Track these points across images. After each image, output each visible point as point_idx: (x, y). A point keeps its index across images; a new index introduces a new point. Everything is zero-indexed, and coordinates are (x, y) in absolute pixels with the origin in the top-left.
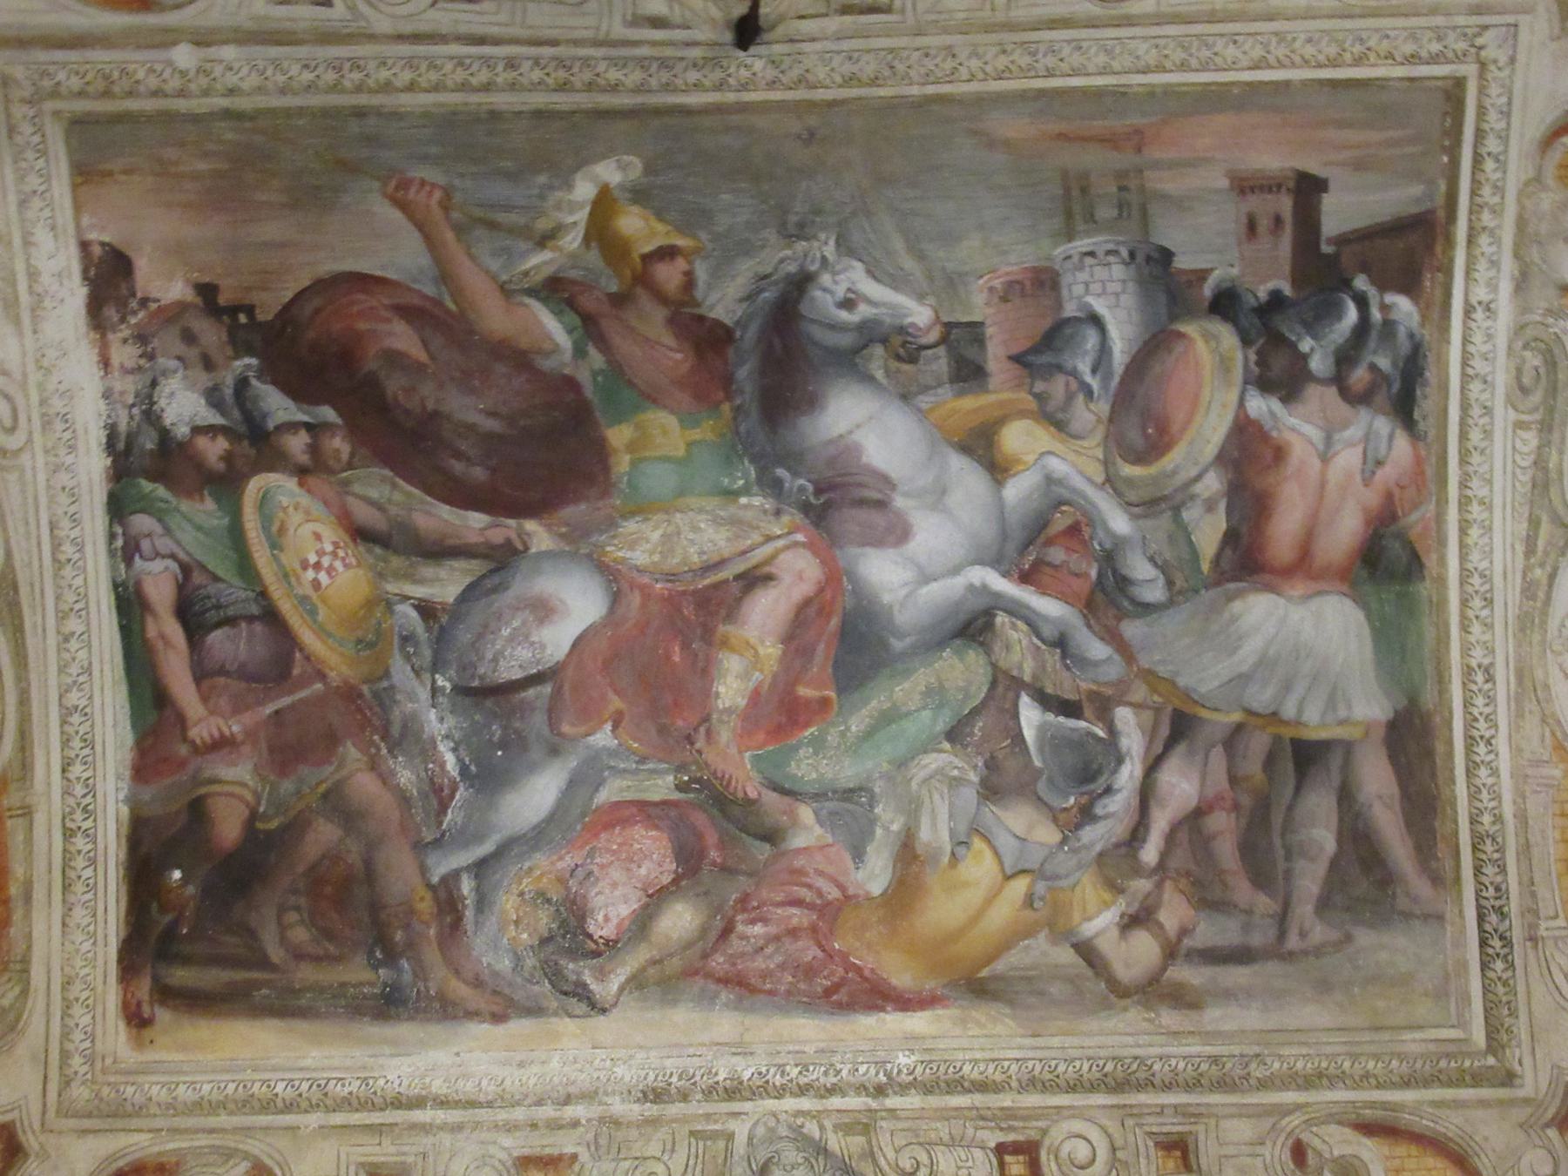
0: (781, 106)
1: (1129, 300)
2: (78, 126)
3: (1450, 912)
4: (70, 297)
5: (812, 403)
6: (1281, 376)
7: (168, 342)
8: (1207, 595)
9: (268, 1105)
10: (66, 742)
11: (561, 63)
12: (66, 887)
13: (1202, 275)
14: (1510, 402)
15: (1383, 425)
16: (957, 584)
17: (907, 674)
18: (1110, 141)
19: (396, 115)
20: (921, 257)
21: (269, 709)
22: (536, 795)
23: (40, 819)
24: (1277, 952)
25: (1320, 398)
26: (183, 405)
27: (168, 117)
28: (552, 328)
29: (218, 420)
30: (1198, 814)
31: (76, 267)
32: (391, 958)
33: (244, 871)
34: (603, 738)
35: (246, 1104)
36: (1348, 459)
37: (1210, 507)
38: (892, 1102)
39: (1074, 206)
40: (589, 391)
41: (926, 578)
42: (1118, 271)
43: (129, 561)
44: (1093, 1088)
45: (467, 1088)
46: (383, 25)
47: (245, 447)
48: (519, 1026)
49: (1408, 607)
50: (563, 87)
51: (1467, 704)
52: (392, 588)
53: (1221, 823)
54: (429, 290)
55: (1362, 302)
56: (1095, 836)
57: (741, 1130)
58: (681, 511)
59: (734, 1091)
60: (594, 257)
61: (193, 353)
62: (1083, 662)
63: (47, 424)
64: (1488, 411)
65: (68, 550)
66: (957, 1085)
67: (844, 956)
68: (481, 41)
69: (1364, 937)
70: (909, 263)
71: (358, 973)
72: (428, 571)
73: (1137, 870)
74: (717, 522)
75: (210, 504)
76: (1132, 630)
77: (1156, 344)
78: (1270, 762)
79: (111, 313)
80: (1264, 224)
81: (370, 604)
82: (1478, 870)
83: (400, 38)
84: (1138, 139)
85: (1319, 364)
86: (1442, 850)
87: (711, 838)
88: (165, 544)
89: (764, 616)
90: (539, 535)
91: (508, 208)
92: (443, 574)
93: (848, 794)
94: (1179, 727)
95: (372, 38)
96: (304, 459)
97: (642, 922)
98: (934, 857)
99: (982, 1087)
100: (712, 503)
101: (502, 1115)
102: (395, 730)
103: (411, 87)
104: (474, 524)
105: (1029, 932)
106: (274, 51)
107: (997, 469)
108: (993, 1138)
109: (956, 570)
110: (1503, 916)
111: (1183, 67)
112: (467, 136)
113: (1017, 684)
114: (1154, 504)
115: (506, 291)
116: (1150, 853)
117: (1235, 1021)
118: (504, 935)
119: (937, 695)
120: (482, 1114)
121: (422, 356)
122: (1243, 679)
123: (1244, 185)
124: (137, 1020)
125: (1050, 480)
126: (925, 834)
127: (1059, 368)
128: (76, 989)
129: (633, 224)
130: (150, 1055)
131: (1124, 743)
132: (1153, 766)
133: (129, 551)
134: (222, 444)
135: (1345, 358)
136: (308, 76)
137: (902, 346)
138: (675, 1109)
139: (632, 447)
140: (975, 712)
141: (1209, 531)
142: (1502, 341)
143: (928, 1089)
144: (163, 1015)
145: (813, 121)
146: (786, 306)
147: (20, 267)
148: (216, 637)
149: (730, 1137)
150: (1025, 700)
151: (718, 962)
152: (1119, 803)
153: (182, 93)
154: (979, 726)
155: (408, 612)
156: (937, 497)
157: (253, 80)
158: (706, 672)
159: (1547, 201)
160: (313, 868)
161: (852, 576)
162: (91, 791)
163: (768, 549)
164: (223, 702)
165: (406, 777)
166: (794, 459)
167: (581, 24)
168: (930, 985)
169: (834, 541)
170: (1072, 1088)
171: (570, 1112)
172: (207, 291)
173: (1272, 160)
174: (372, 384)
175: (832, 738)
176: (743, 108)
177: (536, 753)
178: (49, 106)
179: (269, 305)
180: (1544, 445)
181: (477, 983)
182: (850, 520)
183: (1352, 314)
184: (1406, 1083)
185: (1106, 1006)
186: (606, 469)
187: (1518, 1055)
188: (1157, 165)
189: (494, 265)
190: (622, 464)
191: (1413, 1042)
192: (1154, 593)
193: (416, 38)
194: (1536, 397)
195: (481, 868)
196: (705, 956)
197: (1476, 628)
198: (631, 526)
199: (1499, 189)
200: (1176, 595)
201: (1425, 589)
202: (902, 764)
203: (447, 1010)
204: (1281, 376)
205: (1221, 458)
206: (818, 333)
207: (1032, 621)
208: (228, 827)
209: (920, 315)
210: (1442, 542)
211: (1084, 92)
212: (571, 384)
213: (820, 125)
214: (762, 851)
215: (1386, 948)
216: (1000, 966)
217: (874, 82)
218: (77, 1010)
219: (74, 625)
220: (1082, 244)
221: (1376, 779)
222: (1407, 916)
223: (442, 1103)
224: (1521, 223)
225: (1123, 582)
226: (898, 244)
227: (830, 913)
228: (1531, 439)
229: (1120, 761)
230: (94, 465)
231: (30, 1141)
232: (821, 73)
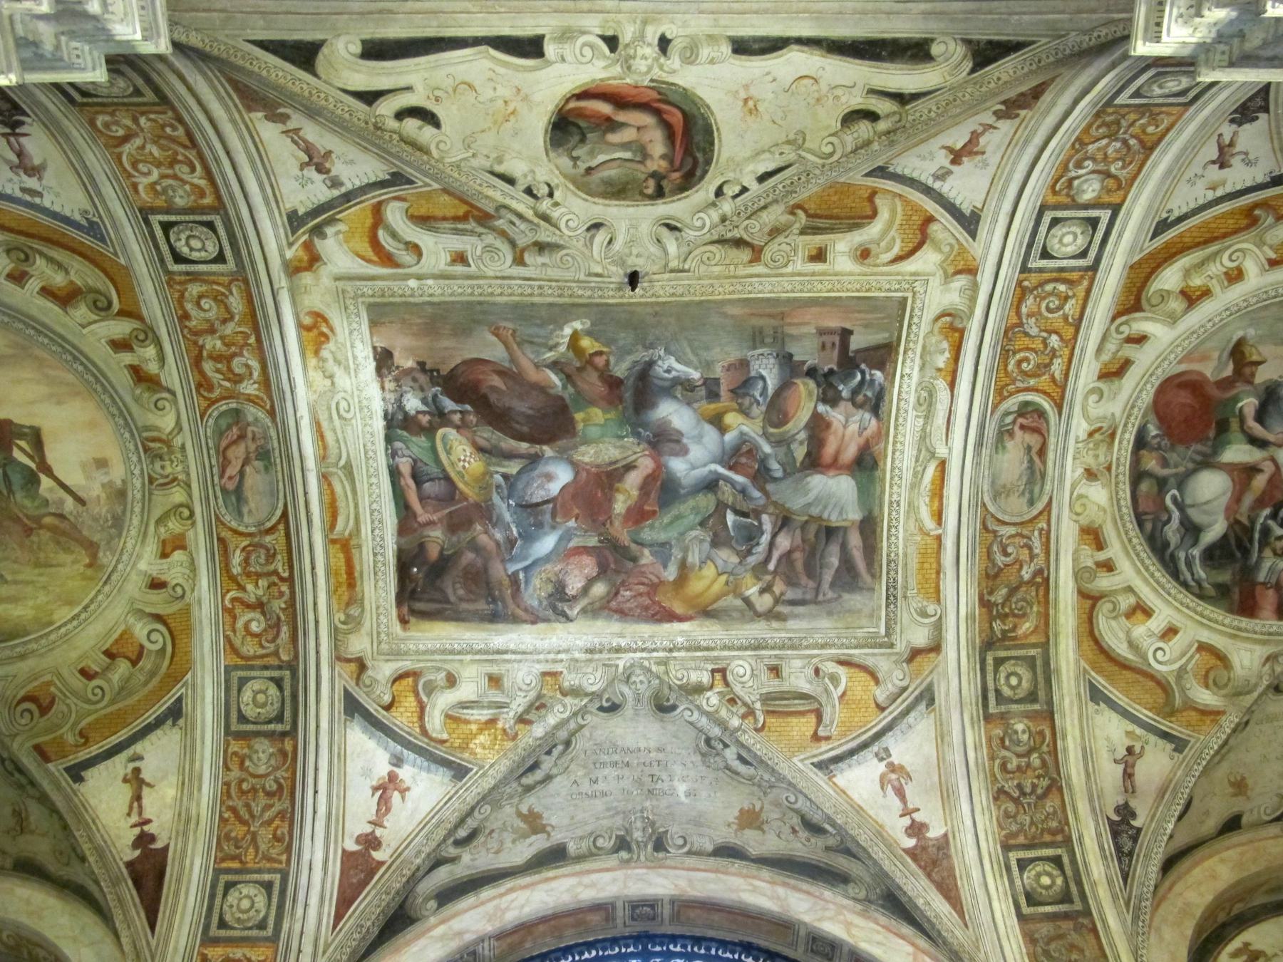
0: (646, 304)
1: (775, 371)
2: (371, 307)
3: (877, 587)
4: (369, 366)
5: (653, 405)
7: (407, 384)
8: (797, 475)
9: (452, 652)
10: (372, 522)
11: (559, 288)
12: (375, 574)
13: (804, 362)
14: (914, 408)
15: (867, 416)
16: (707, 469)
17: (684, 502)
18: (771, 316)
19: (494, 304)
20: (697, 355)
21: (447, 511)
22: (547, 543)
23: (364, 549)
24: (815, 602)
25: (845, 406)
26: (413, 403)
27: (406, 304)
28: (555, 379)
29: (424, 408)
30: (789, 554)
31: (371, 355)
32: (494, 601)
33: (440, 568)
34: (572, 523)
35: (444, 652)
36: (853, 427)
37: (801, 443)
38: (675, 654)
39: (757, 338)
40: (568, 401)
41: (694, 468)
42: (772, 360)
43: (393, 458)
44: (746, 649)
45: (523, 647)
46: (491, 274)
47: (437, 419)
48: (541, 626)
49: (871, 480)
50: (559, 296)
51: (890, 514)
52: (492, 469)
53: (798, 556)
54: (507, 364)
55: (863, 373)
56: (752, 560)
57: (621, 664)
58: (601, 441)
59: (618, 650)
60: (571, 354)
61: (416, 385)
62: (751, 499)
63: (361, 409)
64: (906, 411)
65: (371, 453)
66: (698, 648)
67: (659, 603)
68: (529, 279)
69: (846, 596)
70: (691, 356)
71: (481, 605)
72: (506, 463)
73: (767, 572)
74: (616, 447)
75: (423, 438)
76: (770, 487)
77: (784, 386)
78: (817, 535)
79: (385, 371)
80: (828, 345)
81: (484, 474)
82: (888, 573)
83: (497, 278)
84: (782, 316)
85: (845, 394)
86: (876, 566)
87: (611, 559)
88: (407, 452)
89: (633, 480)
90: (548, 451)
91: (538, 337)
92: (512, 463)
93: (663, 545)
94: (784, 522)
95: (485, 277)
96: (459, 423)
97: (585, 590)
98: (693, 566)
99: (708, 649)
100: (614, 440)
101: (536, 657)
102: (494, 519)
103: (501, 294)
104: (524, 446)
105: (725, 594)
106: (447, 282)
108: (710, 667)
109: (705, 465)
110: (895, 589)
111: (801, 291)
112: (524, 312)
113: (727, 506)
114: (780, 442)
115: (537, 366)
116: (771, 567)
117: (797, 626)
118: (536, 592)
119: (695, 510)
120: (529, 657)
121: (504, 388)
122: (809, 505)
123: (822, 332)
124: (404, 621)
125: (742, 434)
126: (690, 559)
127: (748, 394)
128: (381, 610)
129: (586, 343)
130: (408, 634)
131: (764, 527)
132: (774, 536)
133: (394, 454)
134: (427, 418)
135: (855, 392)
136: (460, 290)
137: (687, 386)
138: (597, 656)
139: (584, 420)
140: (710, 516)
141: (800, 452)
142: (913, 388)
143: (688, 649)
144: (413, 620)
145: (657, 309)
146: (644, 374)
147: (350, 354)
148: (427, 485)
149: (617, 666)
150: (729, 511)
151: (613, 604)
153: (412, 296)
155: (498, 478)
156: (699, 438)
157: (440, 291)
158: (610, 500)
159: (934, 340)
160: (465, 568)
161: (666, 467)
162: (382, 539)
163: (634, 457)
164: (430, 508)
165: (499, 536)
166: (645, 425)
167: (569, 275)
168: (690, 612)
169: (660, 454)
170: (739, 649)
171: (560, 656)
172: (422, 365)
173: (834, 323)
174: (485, 397)
175: (657, 524)
176: (630, 304)
177: (547, 528)
178: (360, 300)
179: (445, 370)
180: (925, 424)
181: (526, 610)
182: (668, 447)
183: (859, 377)
184: (856, 647)
185: (752, 620)
186: (574, 428)
187: (896, 638)
188: (790, 324)
189: (532, 356)
190: (580, 426)
191: (860, 633)
192: (779, 474)
193: (503, 278)
194: (924, 407)
195: (526, 569)
196: (608, 602)
197: (895, 488)
198: (583, 448)
199: (917, 335)
200: (787, 474)
201: (878, 473)
202: (682, 534)
203: (515, 620)
204: (831, 399)
205: (807, 426)
206: (656, 381)
207: (732, 483)
208: (433, 552)
209: (695, 375)
210: (886, 457)
211: (762, 299)
212: (562, 399)
213: (660, 310)
214: (630, 565)
215: (854, 600)
216: (715, 606)
217: (682, 295)
218: (382, 617)
219: (374, 480)
220: (760, 351)
221: (855, 540)
222: (861, 589)
223: (514, 652)
224: (924, 347)
225: (768, 470)
226: (688, 350)
227: (655, 587)
228: (921, 421)
229: (762, 533)
230: (379, 425)
231: (369, 663)
232: (661, 293)
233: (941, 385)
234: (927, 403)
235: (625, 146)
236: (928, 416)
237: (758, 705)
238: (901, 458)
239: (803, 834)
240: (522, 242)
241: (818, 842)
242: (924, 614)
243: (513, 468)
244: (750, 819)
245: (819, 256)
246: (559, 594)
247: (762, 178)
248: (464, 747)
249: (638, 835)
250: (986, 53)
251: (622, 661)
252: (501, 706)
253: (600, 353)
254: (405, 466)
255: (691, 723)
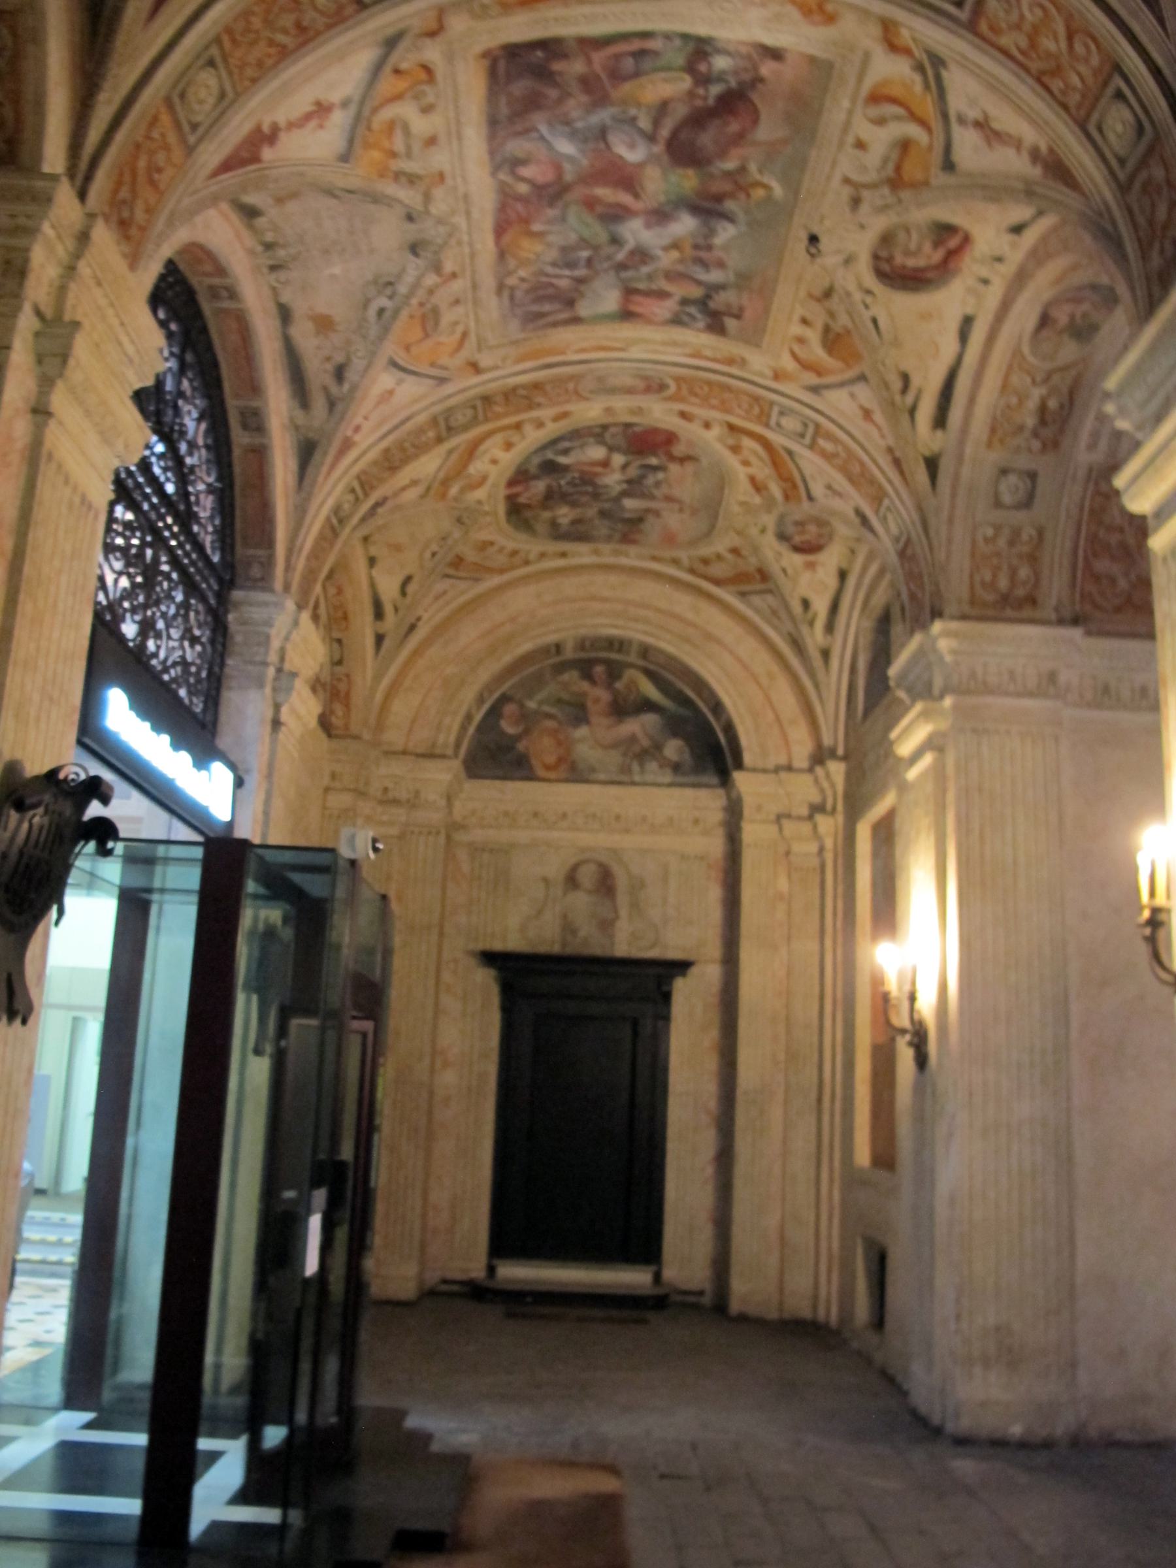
4: (769, 40)
6: (685, 302)
22: (566, 147)
26: (721, 63)
28: (730, 165)
30: (552, 285)
33: (543, 74)
48: (486, 157)
53: (550, 291)
59: (468, 213)
71: (504, 110)
77: (699, 283)
89: (626, 198)
90: (659, 149)
94: (580, 281)
107: (666, 249)
112: (800, 164)
114: (650, 277)
118: (516, 147)
123: (741, 309)
124: (486, 54)
129: (759, 193)
133: (668, 36)
152: (558, 271)
154: (584, 243)
172: (761, 80)
173: (748, 314)
179: (755, 97)
195: (542, 138)
208: (557, 66)
215: (514, 325)
227: (526, 221)
233: (688, 351)
234: (675, 344)
235: (920, 248)
236: (664, 343)
237: (429, 306)
238: (627, 331)
239: (329, 367)
240: (866, 194)
241: (329, 381)
242: (504, 359)
243: (644, 123)
244: (324, 324)
245: (804, 321)
246: (516, 163)
247: (875, 321)
248: (367, 146)
249: (281, 253)
250: (932, 464)
251: (460, 221)
252: (409, 155)
253: (748, 195)
254: (655, 44)
255: (403, 270)
